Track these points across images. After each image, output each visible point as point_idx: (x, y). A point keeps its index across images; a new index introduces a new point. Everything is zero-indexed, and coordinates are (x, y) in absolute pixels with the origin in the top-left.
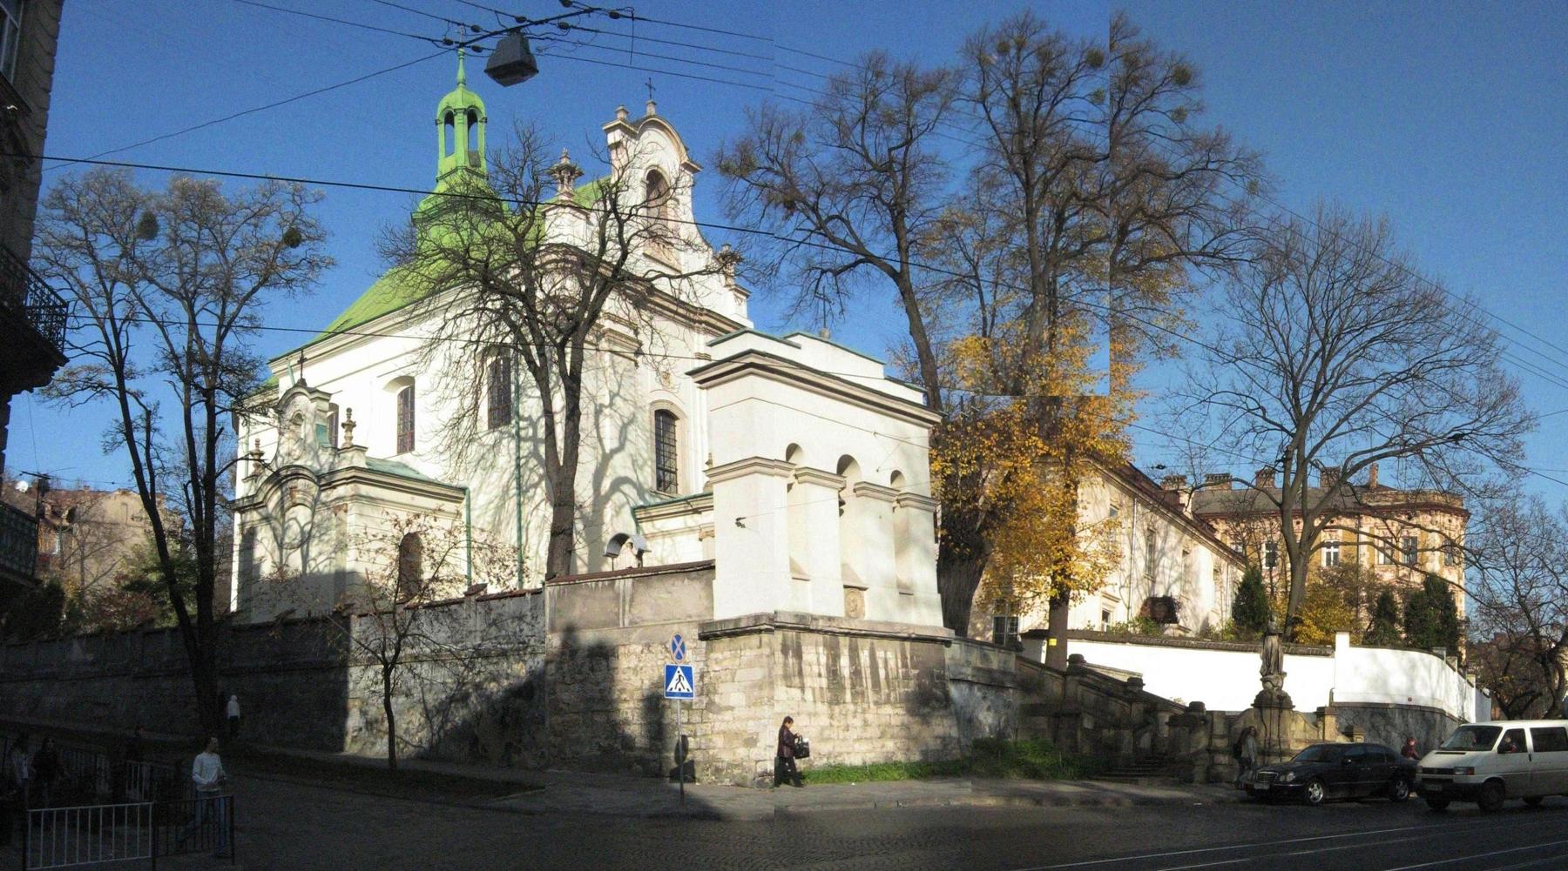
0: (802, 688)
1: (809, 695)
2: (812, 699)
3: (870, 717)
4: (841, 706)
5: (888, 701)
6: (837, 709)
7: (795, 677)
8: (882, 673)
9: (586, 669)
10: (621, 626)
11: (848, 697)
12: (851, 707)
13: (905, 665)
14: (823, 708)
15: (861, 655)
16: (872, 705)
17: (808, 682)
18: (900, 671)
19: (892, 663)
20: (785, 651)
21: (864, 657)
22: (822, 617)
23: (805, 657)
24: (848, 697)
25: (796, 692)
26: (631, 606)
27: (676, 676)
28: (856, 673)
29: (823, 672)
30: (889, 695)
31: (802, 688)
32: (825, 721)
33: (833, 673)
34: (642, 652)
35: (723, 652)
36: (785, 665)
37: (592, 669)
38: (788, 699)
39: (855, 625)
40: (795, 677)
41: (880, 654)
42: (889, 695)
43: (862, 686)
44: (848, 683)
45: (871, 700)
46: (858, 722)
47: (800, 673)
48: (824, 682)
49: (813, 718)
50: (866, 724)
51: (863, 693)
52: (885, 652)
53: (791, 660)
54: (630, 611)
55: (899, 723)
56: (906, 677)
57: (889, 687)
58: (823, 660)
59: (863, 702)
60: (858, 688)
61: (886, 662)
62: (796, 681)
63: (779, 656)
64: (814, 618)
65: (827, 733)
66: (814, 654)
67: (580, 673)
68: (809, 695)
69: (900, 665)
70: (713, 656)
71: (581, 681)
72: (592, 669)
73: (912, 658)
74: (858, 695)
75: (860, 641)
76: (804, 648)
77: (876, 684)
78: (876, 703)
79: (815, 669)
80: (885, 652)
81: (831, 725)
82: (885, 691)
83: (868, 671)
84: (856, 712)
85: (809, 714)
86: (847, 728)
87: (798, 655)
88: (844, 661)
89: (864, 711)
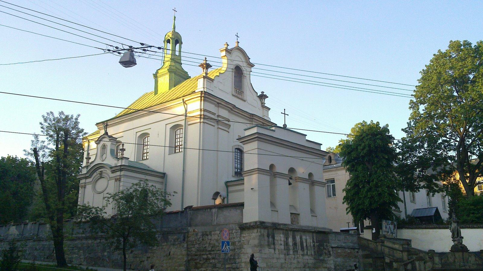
0: (275, 249)
3: (299, 260)
4: (289, 256)
5: (307, 254)
6: (287, 257)
7: (272, 244)
8: (305, 244)
9: (201, 239)
10: (213, 224)
11: (291, 252)
12: (293, 256)
13: (313, 242)
14: (282, 256)
15: (297, 237)
16: (301, 256)
17: (277, 247)
18: (312, 244)
19: (308, 241)
20: (268, 236)
22: (282, 224)
23: (276, 238)
24: (291, 252)
25: (272, 251)
26: (217, 218)
27: (225, 245)
28: (295, 244)
29: (282, 243)
30: (307, 252)
31: (275, 249)
32: (283, 261)
33: (286, 244)
34: (220, 234)
35: (246, 234)
36: (268, 241)
37: (203, 240)
39: (295, 227)
40: (272, 244)
41: (304, 237)
42: (307, 252)
43: (297, 248)
44: (291, 248)
46: (295, 261)
47: (274, 244)
48: (282, 247)
49: (278, 260)
50: (298, 262)
51: (297, 251)
52: (306, 237)
53: (271, 239)
54: (216, 220)
55: (311, 262)
56: (314, 246)
57: (307, 249)
58: (283, 239)
59: (297, 254)
61: (306, 240)
62: (272, 246)
63: (266, 238)
64: (279, 225)
66: (280, 237)
67: (199, 241)
68: (277, 251)
69: (311, 241)
70: (243, 235)
71: (199, 244)
72: (203, 240)
73: (316, 239)
74: (295, 251)
75: (296, 233)
76: (276, 235)
78: (303, 255)
79: (280, 242)
80: (306, 237)
81: (286, 263)
82: (305, 251)
83: (300, 245)
84: (295, 258)
85: (277, 259)
86: (291, 263)
87: (273, 237)
88: (290, 240)
89: (298, 258)
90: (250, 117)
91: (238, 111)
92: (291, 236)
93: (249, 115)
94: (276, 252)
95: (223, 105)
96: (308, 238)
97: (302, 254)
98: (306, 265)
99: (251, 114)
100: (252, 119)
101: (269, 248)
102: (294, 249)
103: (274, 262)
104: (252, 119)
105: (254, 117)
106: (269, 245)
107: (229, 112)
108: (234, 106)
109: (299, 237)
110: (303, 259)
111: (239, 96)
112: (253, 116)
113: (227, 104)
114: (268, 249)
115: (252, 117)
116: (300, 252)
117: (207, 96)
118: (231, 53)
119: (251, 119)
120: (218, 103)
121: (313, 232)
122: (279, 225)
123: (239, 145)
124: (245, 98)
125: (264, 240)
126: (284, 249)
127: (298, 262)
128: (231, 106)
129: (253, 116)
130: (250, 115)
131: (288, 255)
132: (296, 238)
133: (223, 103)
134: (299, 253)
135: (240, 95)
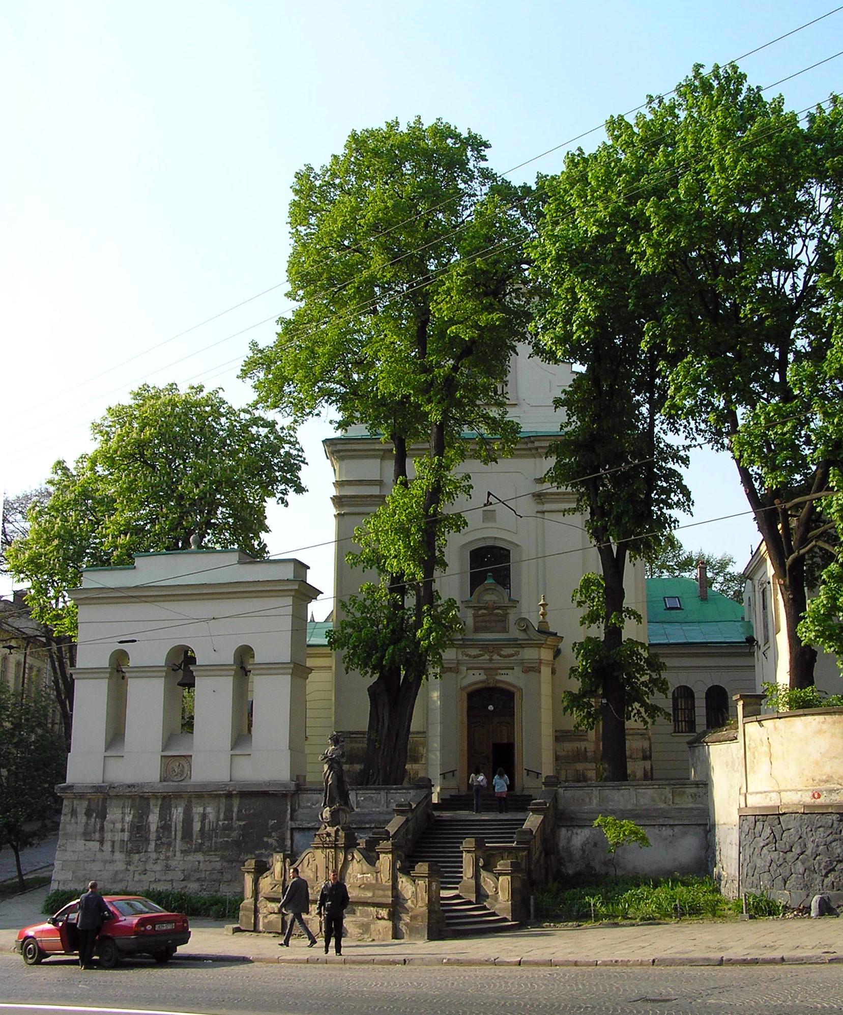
0: (102, 842)
1: (107, 847)
2: (110, 850)
3: (173, 863)
6: (137, 857)
8: (197, 826)
12: (154, 856)
13: (228, 817)
15: (174, 810)
16: (178, 854)
17: (108, 836)
20: (88, 814)
21: (178, 813)
24: (152, 846)
25: (97, 844)
28: (165, 827)
31: (102, 842)
32: (121, 866)
38: (85, 850)
41: (198, 810)
44: (153, 836)
45: (177, 849)
46: (158, 867)
47: (102, 829)
48: (126, 836)
49: (107, 865)
50: (167, 868)
60: (164, 840)
61: (204, 816)
63: (82, 819)
65: (121, 876)
68: (107, 847)
73: (239, 811)
77: (187, 834)
79: (119, 826)
85: (105, 862)
86: (145, 872)
89: (167, 858)
92: (157, 810)
94: (104, 848)
96: (209, 810)
97: (183, 849)
98: (190, 875)
101: (88, 838)
102: (158, 838)
103: (94, 869)
106: (87, 835)
109: (180, 810)
110: (183, 860)
114: (83, 842)
115: (530, 445)
116: (179, 845)
117: (339, 447)
121: (229, 795)
122: (114, 788)
123: (484, 538)
125: (77, 823)
126: (130, 840)
127: (167, 868)
129: (533, 442)
131: (139, 852)
132: (170, 812)
134: (175, 847)
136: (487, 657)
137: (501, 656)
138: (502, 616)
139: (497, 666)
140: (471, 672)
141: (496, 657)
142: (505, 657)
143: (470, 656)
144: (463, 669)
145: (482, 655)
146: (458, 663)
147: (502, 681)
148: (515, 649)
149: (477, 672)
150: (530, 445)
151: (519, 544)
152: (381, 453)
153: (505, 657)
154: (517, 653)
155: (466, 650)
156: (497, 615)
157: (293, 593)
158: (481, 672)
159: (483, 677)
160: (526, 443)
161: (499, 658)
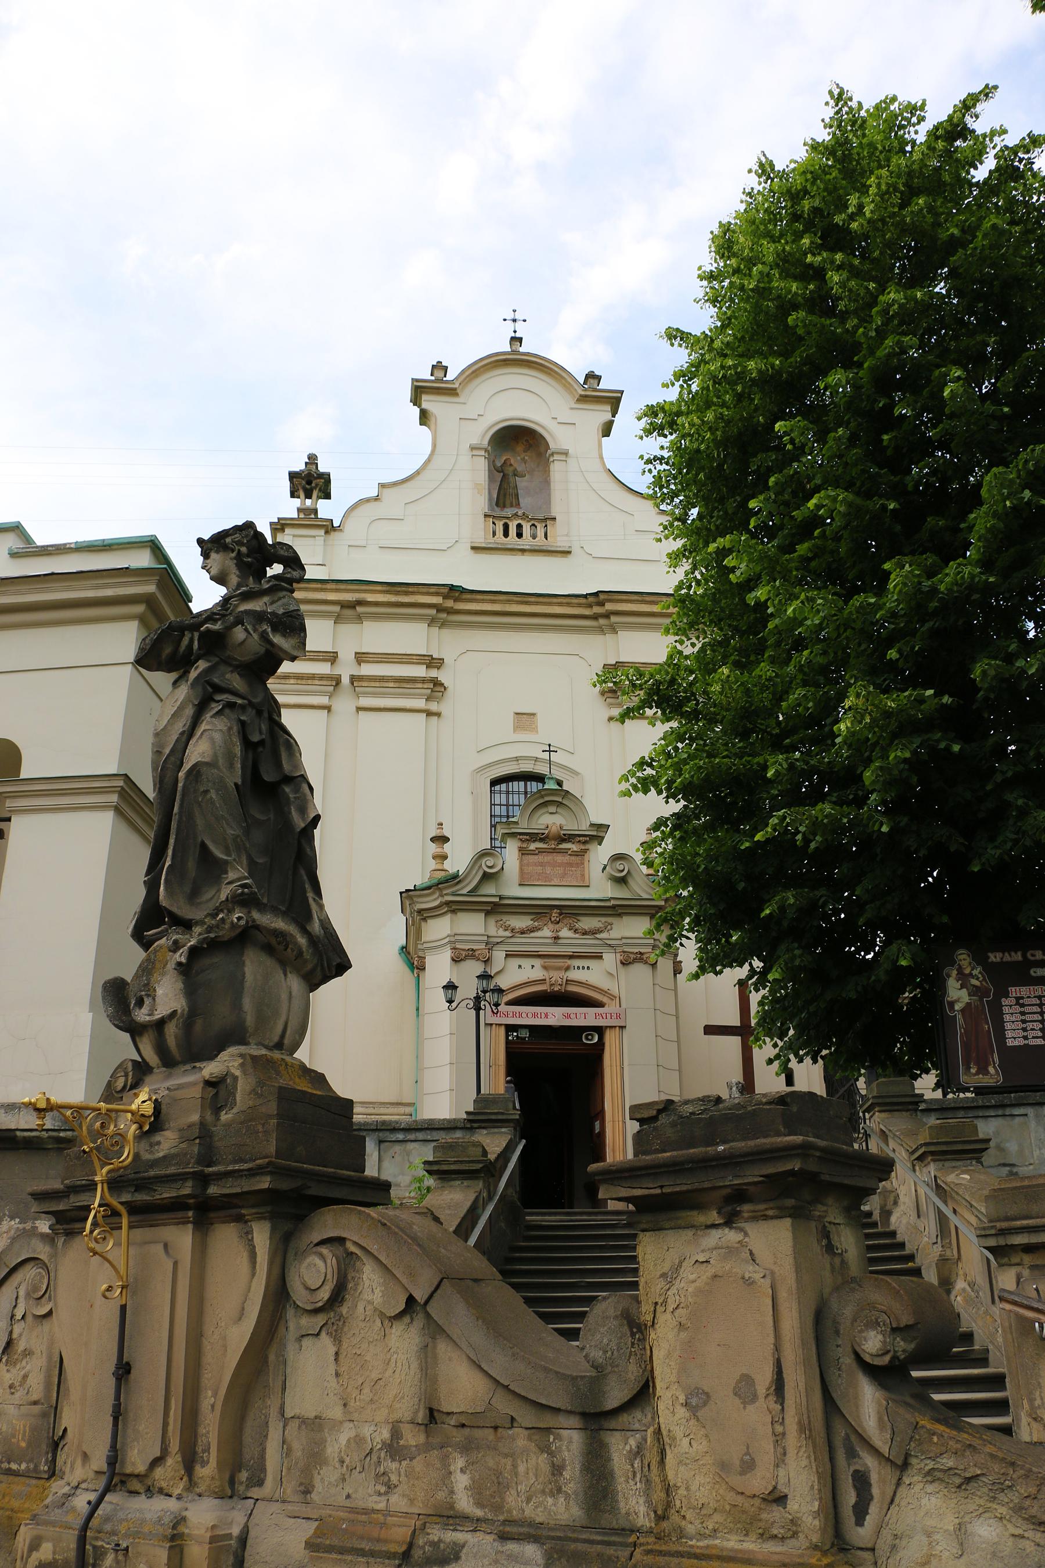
90: (587, 612)
91: (497, 607)
93: (579, 605)
95: (376, 604)
99: (585, 596)
100: (607, 615)
104: (607, 615)
105: (609, 606)
107: (432, 622)
108: (446, 590)
111: (527, 541)
112: (602, 604)
113: (397, 593)
115: (597, 610)
118: (455, 389)
119: (602, 621)
120: (352, 605)
123: (517, 759)
124: (561, 543)
128: (437, 594)
129: (602, 604)
130: (583, 601)
133: (370, 597)
135: (534, 537)
136: (546, 932)
137: (576, 931)
138: (576, 854)
139: (570, 950)
140: (514, 962)
141: (565, 933)
142: (585, 933)
143: (512, 930)
144: (499, 955)
145: (538, 929)
146: (490, 945)
147: (579, 983)
148: (603, 919)
149: (526, 963)
150: (597, 610)
151: (578, 771)
152: (337, 608)
153: (585, 933)
154: (607, 927)
155: (505, 918)
156: (565, 851)
157: (140, 609)
158: (537, 963)
159: (538, 973)
160: (590, 606)
161: (570, 934)
